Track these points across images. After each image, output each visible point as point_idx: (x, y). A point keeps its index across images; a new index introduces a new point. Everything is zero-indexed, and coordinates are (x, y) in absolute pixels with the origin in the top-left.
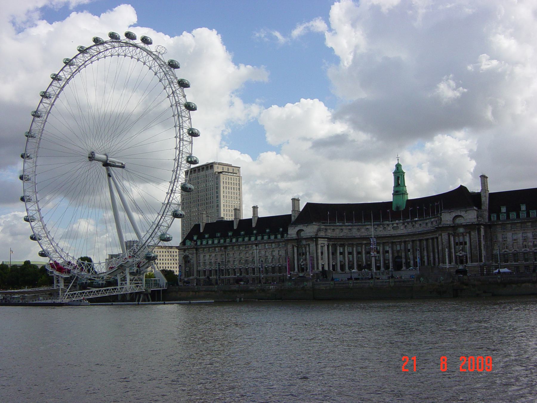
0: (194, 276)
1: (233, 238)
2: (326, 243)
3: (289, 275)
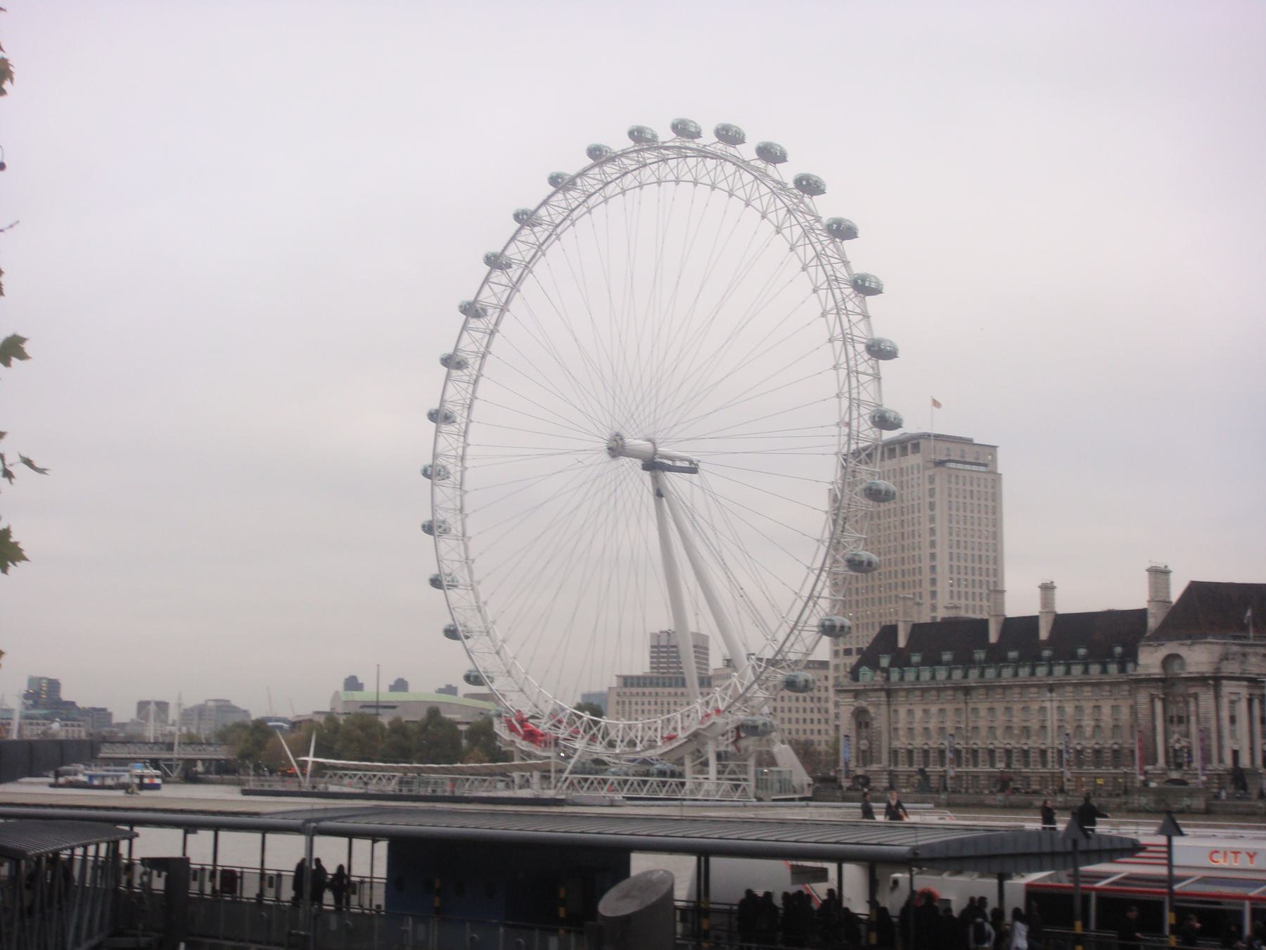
0: (881, 763)
3: (1142, 778)
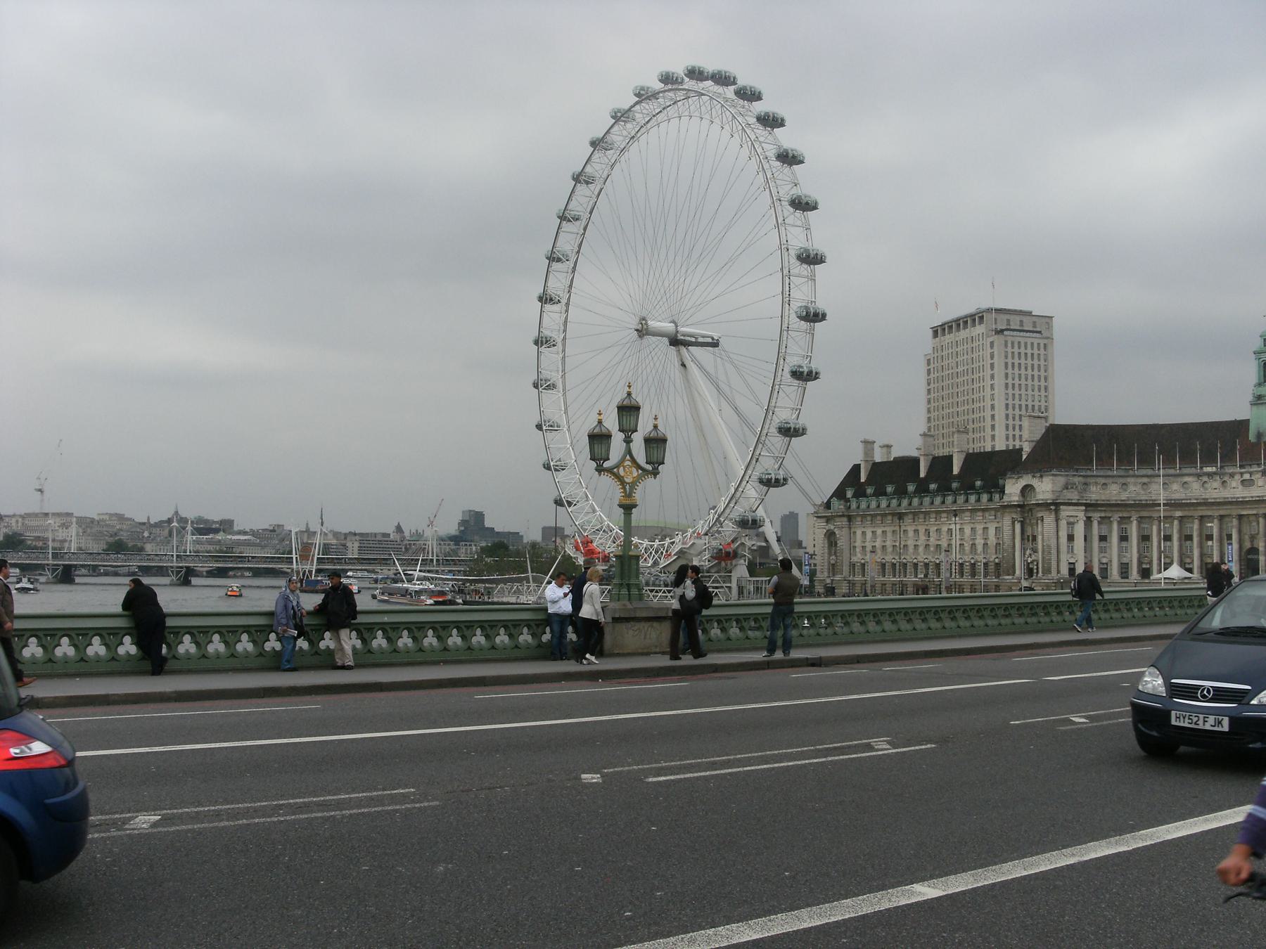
1: (912, 497)
2: (1081, 515)
